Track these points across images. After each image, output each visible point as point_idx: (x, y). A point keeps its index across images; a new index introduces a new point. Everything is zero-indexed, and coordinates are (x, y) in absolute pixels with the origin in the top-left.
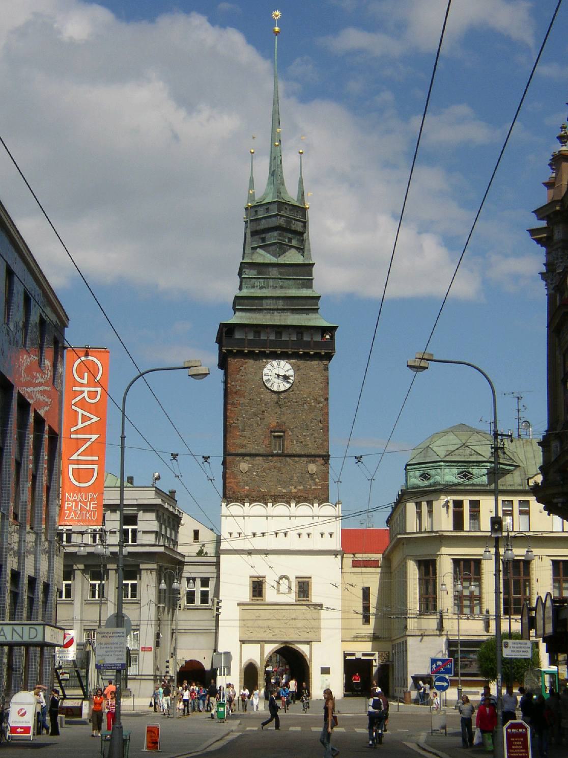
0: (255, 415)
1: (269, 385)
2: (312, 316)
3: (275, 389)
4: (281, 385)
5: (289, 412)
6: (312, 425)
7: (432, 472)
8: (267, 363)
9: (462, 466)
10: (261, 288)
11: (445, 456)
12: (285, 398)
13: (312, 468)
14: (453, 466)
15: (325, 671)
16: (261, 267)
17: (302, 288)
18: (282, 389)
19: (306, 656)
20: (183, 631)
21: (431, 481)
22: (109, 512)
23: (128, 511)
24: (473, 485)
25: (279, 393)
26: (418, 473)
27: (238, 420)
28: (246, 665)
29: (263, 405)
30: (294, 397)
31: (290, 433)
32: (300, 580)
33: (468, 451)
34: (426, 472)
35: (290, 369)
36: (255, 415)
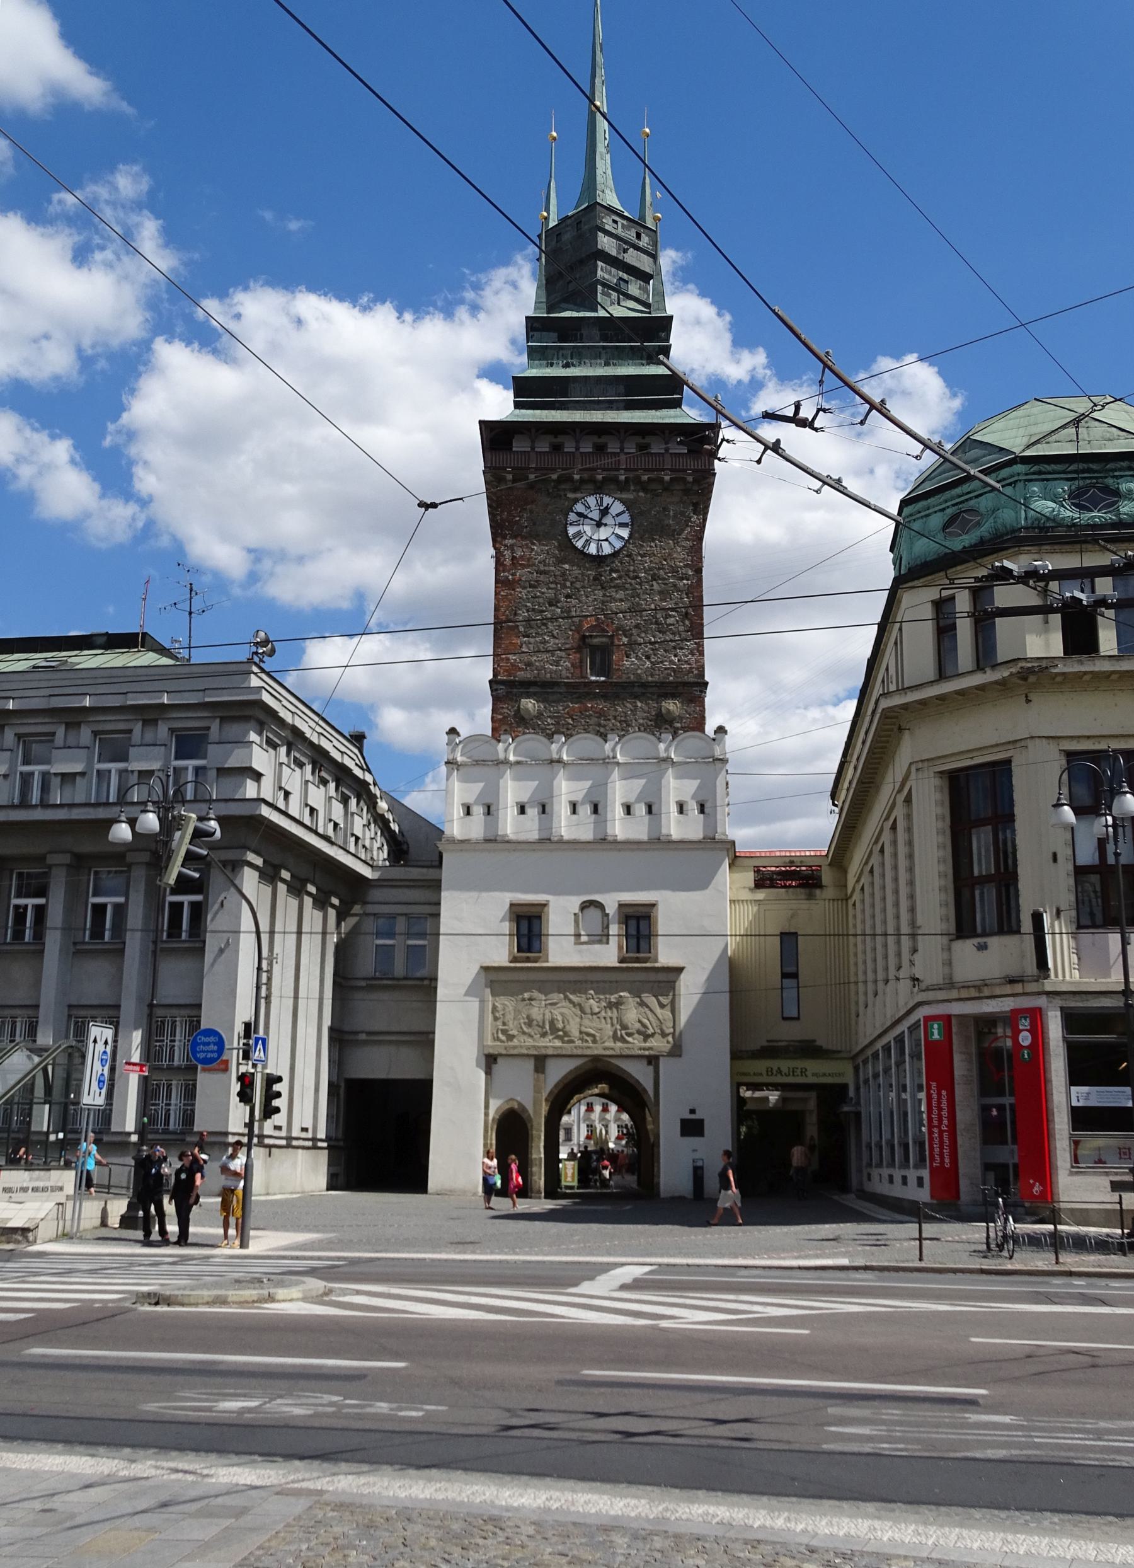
0: (552, 603)
1: (579, 544)
2: (672, 412)
3: (592, 550)
4: (605, 544)
5: (621, 594)
6: (669, 621)
7: (985, 503)
8: (576, 501)
9: (1083, 471)
10: (567, 366)
11: (1028, 447)
12: (612, 571)
13: (672, 706)
14: (1054, 472)
15: (692, 1127)
16: (567, 330)
17: (648, 364)
18: (607, 550)
19: (645, 1090)
20: (363, 1037)
21: (985, 530)
22: (140, 724)
23: (189, 722)
24: (1119, 524)
25: (599, 560)
26: (936, 521)
27: (516, 614)
28: (501, 1112)
29: (568, 584)
30: (632, 568)
31: (625, 640)
32: (630, 910)
33: (1098, 430)
34: (964, 506)
35: (623, 512)
36: (552, 603)
